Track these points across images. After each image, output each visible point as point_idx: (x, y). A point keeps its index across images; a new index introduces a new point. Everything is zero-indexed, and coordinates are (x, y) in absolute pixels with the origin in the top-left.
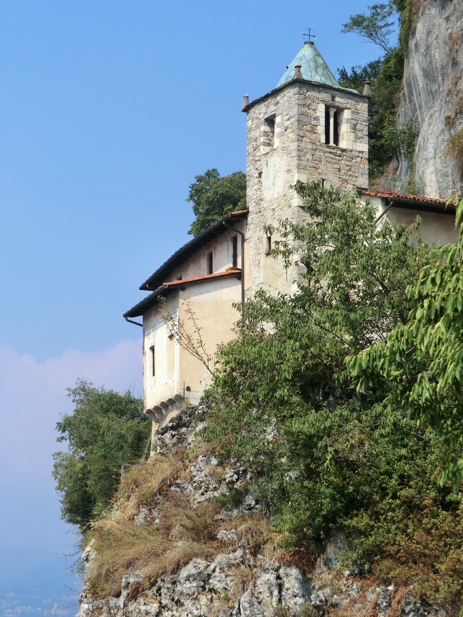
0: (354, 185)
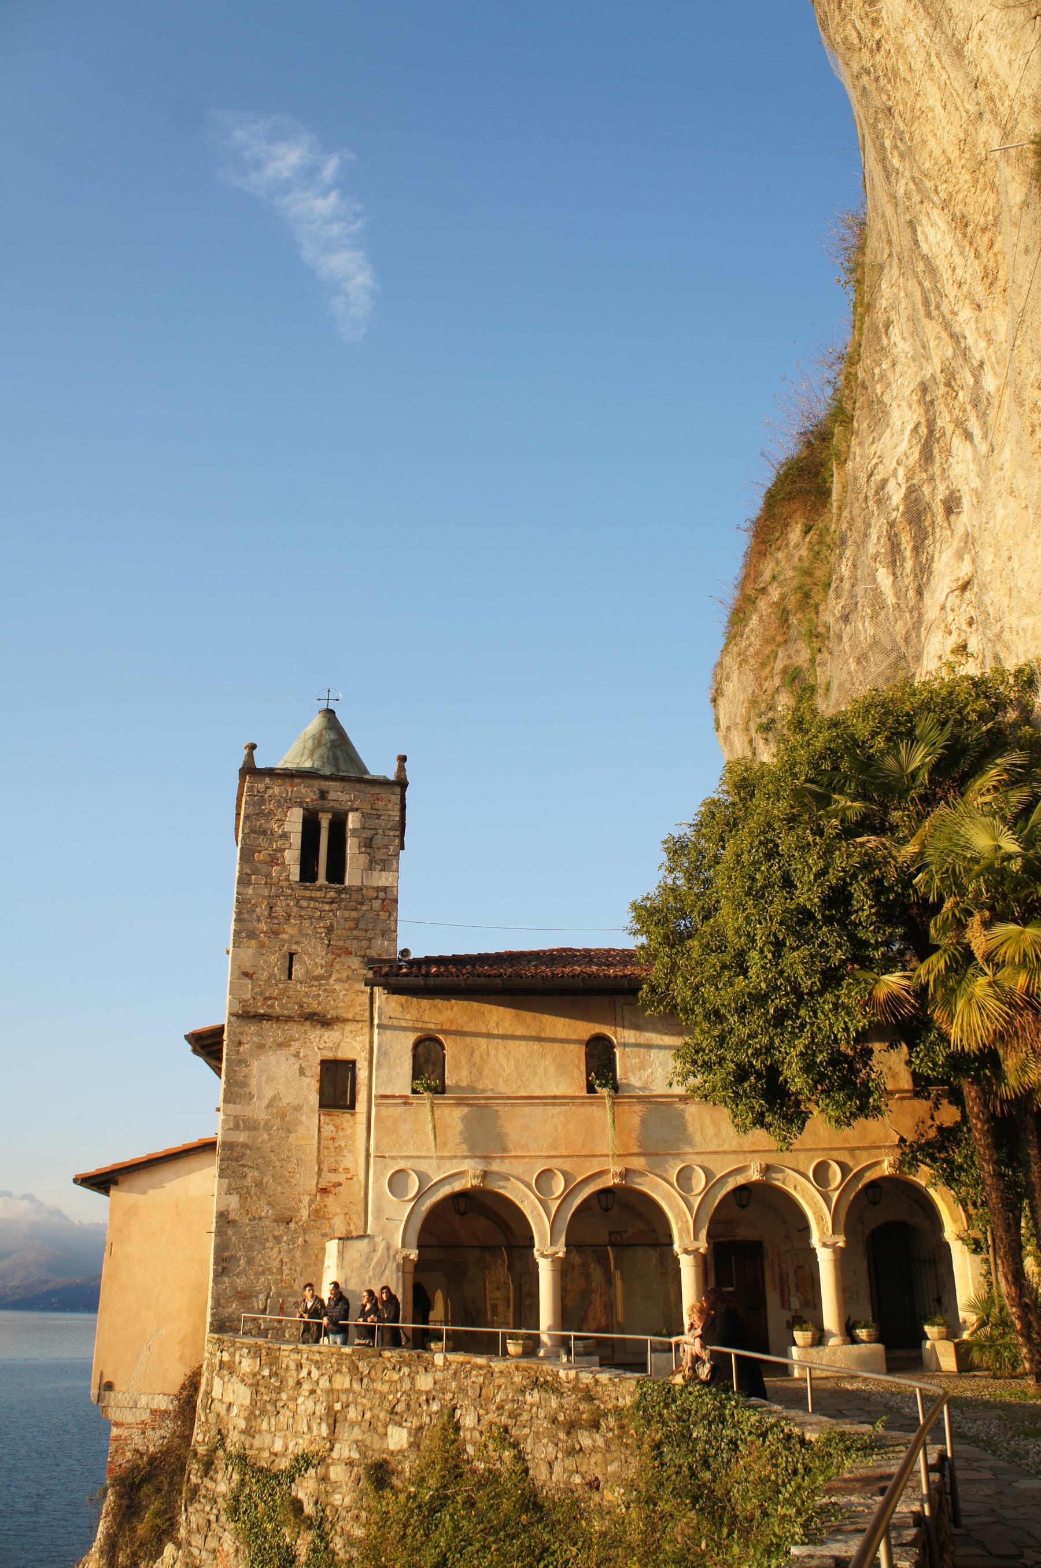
0: (363, 957)
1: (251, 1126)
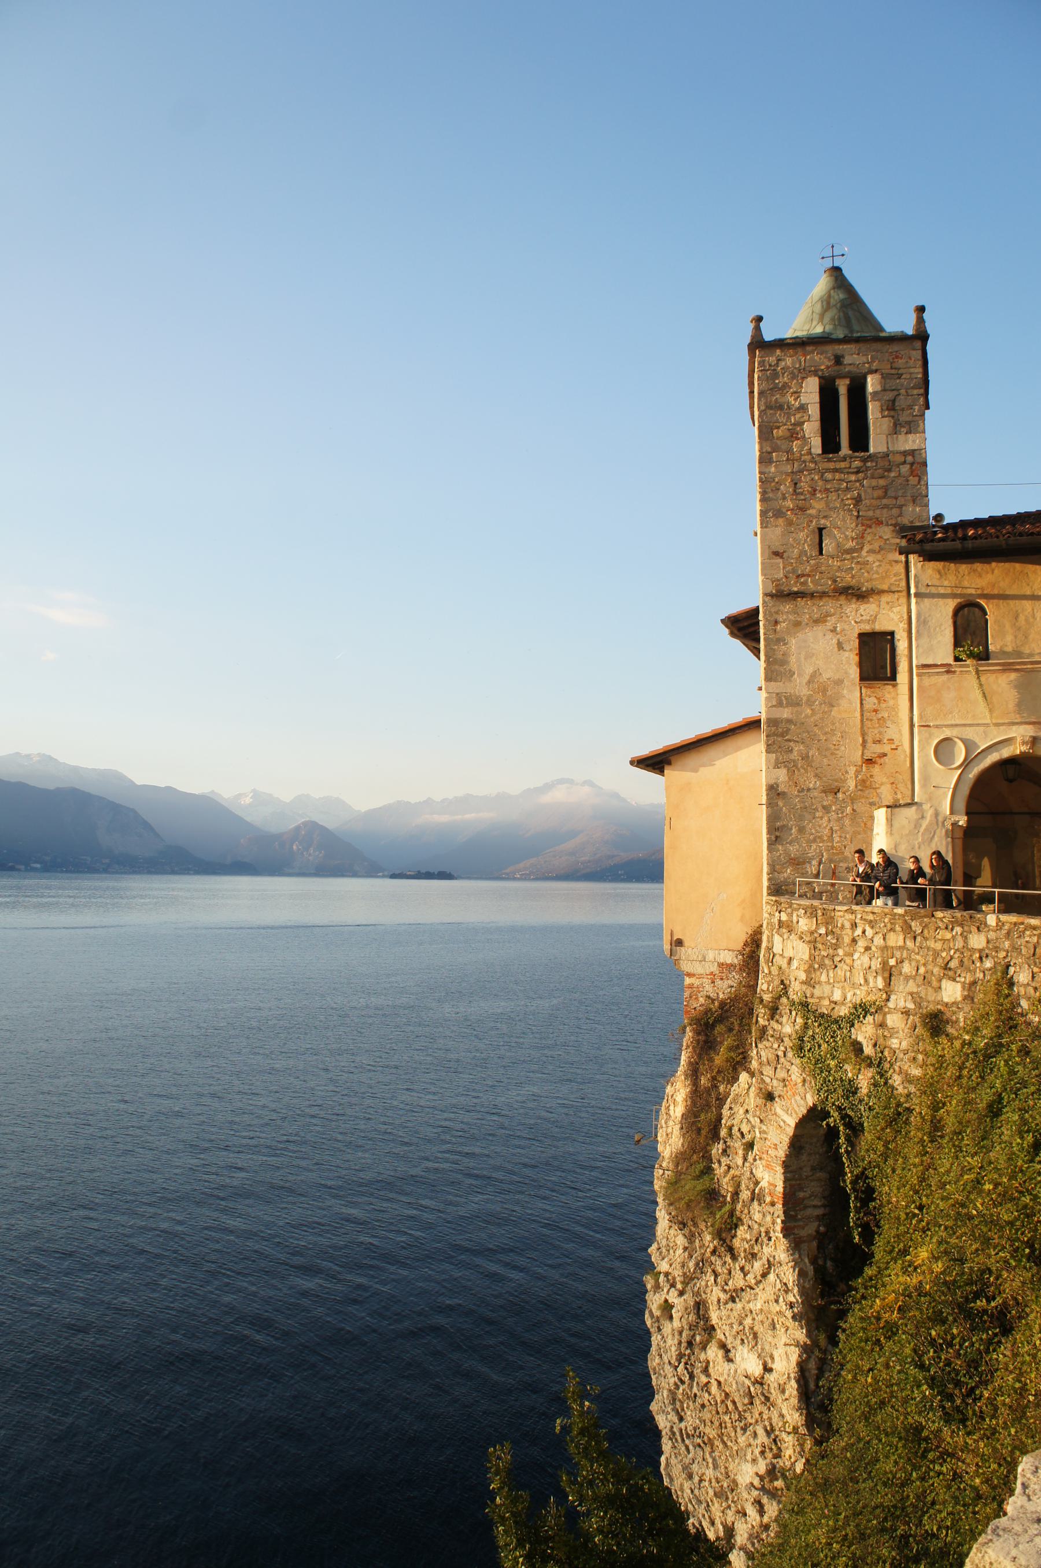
0: (895, 525)
1: (793, 702)
